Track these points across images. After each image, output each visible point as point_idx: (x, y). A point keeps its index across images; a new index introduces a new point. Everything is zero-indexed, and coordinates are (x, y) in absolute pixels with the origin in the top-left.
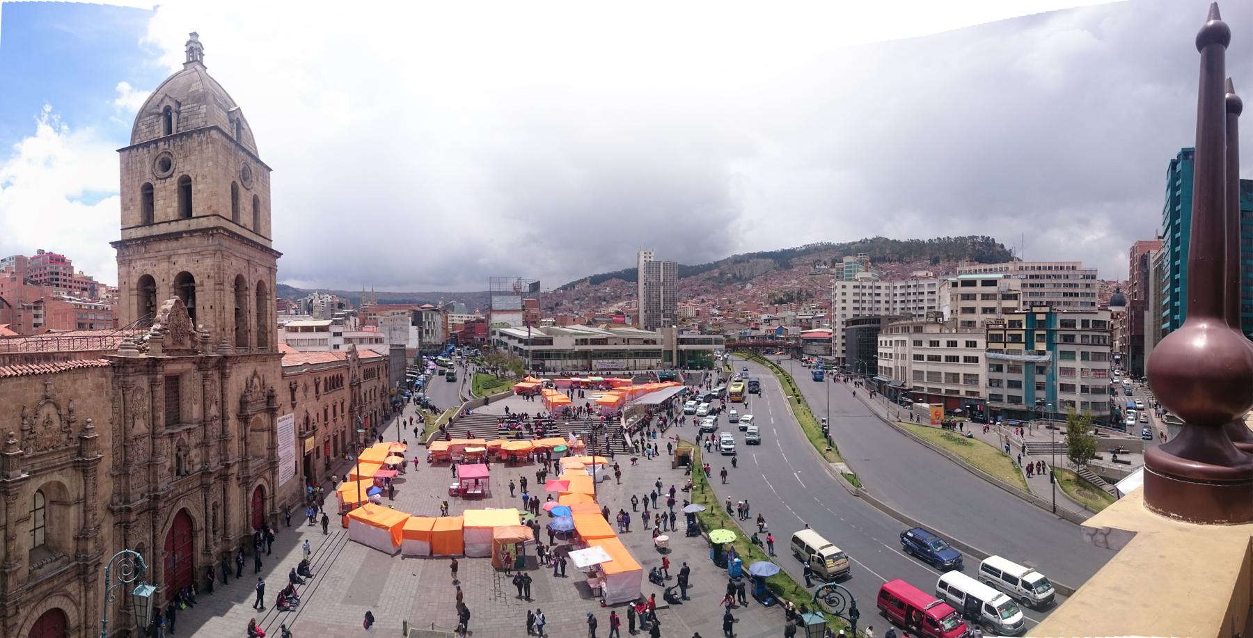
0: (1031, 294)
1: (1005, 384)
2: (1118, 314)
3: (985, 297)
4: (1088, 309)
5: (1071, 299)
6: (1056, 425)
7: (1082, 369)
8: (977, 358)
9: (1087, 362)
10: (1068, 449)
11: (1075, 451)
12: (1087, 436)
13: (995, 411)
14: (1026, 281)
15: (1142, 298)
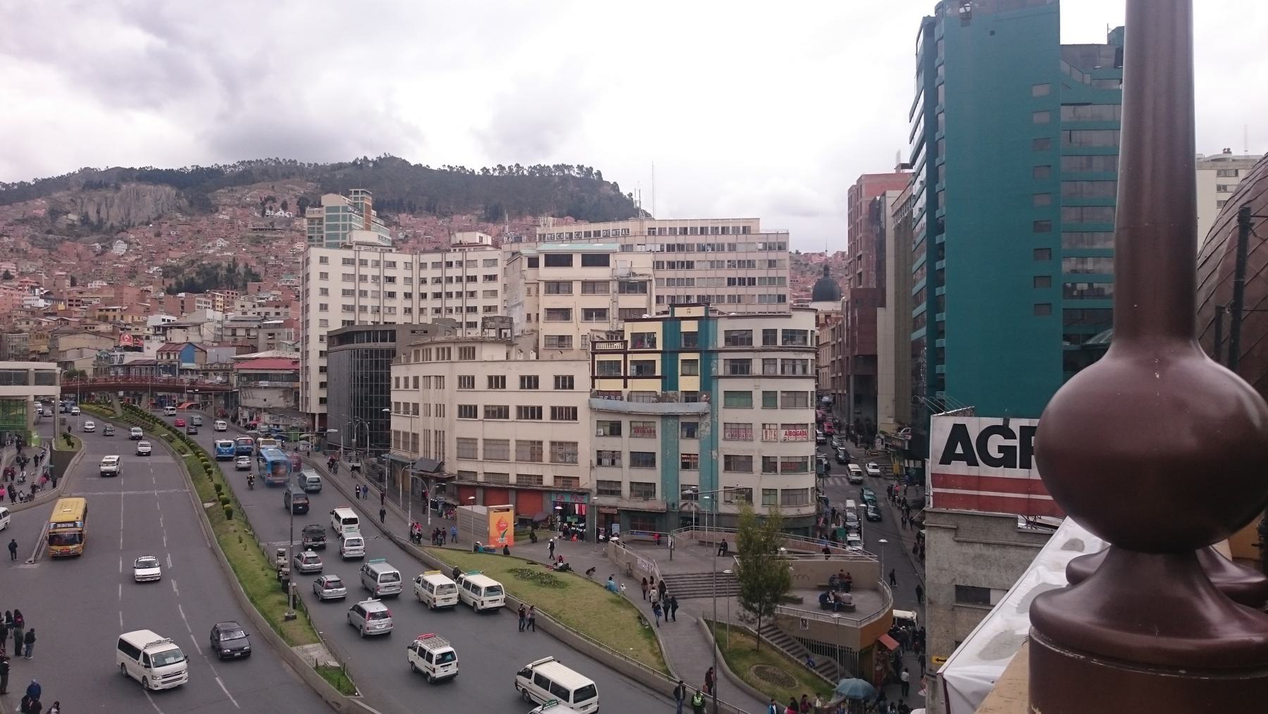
1: (626, 459)
2: (828, 316)
3: (590, 287)
4: (773, 308)
5: (741, 290)
7: (764, 425)
13: (607, 515)
14: (661, 257)
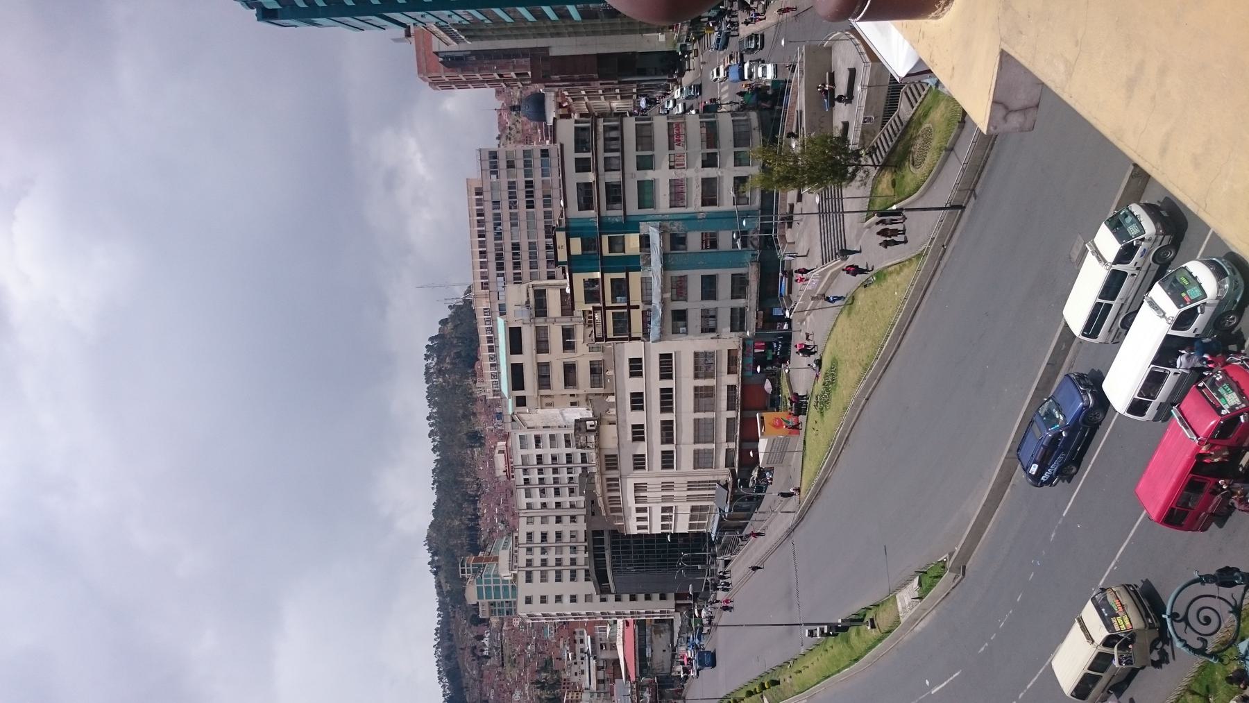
0: (533, 266)
1: (709, 304)
2: (560, 106)
3: (542, 345)
4: (554, 161)
6: (783, 210)
7: (671, 167)
8: (662, 356)
9: (657, 160)
10: (831, 187)
11: (835, 174)
12: (803, 153)
15: (526, 61)
